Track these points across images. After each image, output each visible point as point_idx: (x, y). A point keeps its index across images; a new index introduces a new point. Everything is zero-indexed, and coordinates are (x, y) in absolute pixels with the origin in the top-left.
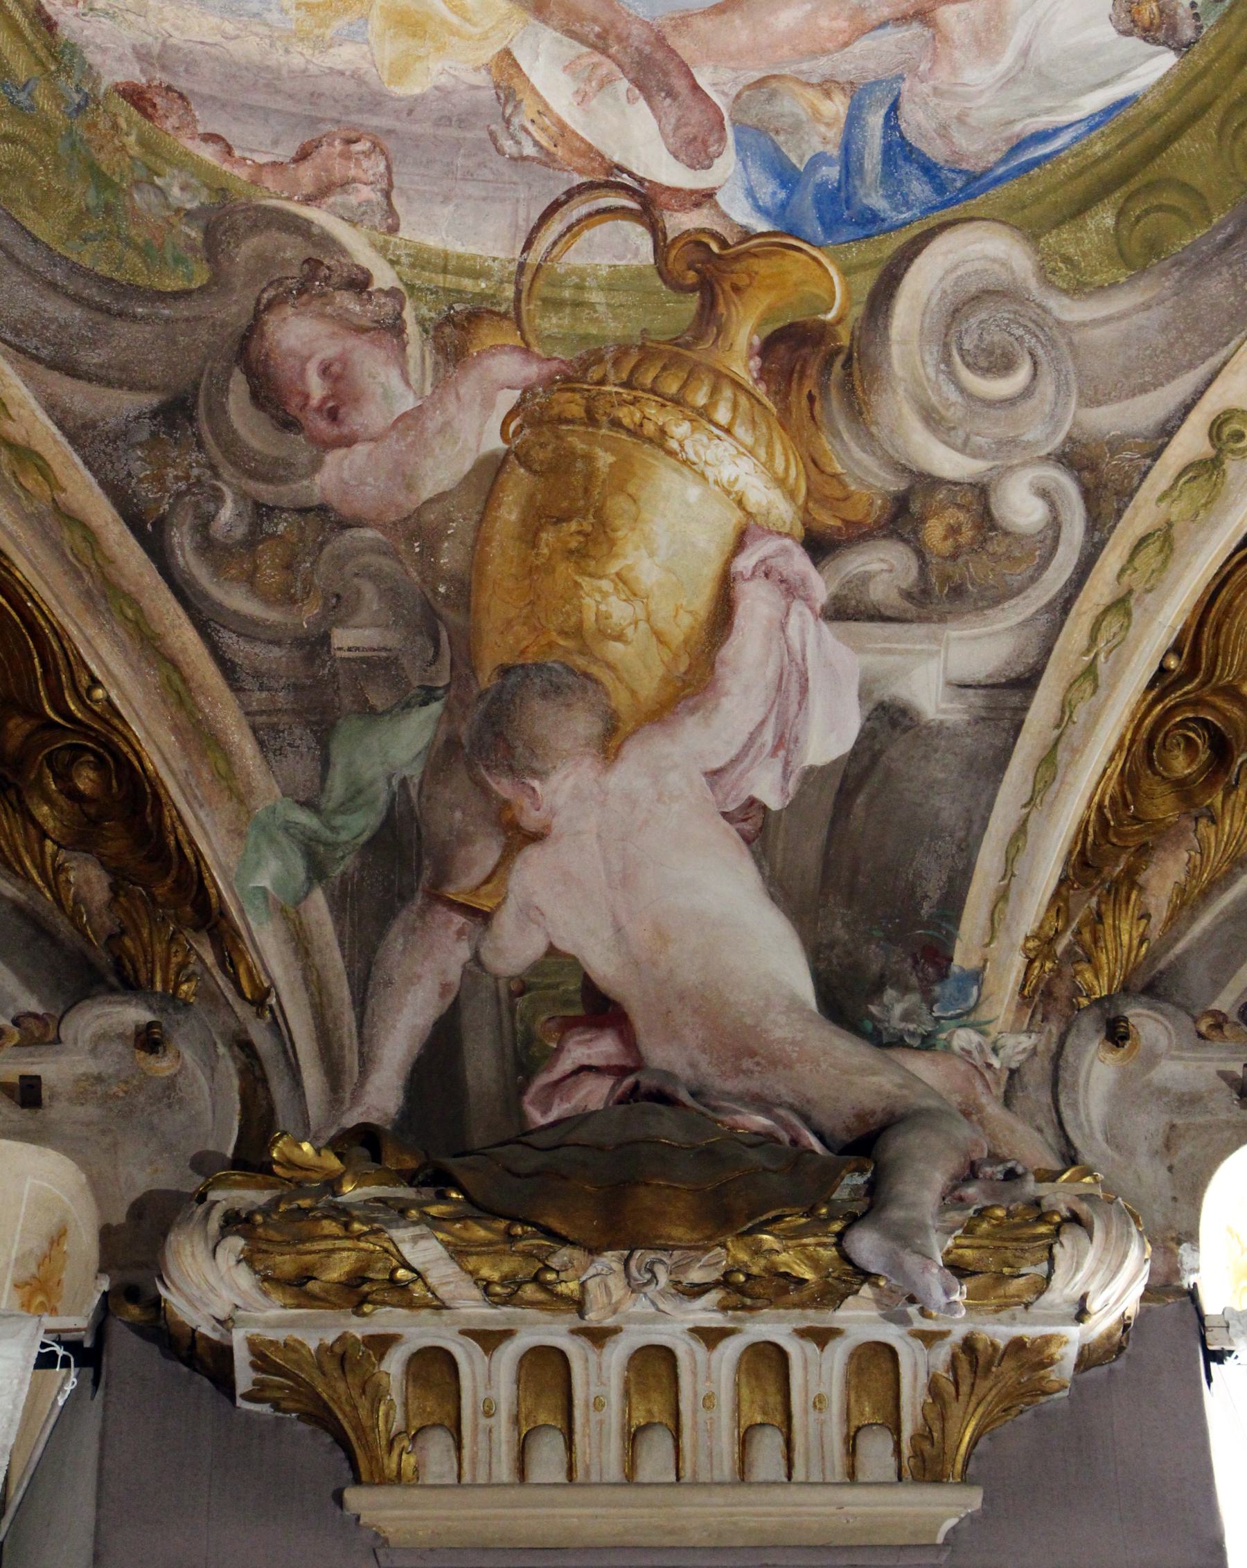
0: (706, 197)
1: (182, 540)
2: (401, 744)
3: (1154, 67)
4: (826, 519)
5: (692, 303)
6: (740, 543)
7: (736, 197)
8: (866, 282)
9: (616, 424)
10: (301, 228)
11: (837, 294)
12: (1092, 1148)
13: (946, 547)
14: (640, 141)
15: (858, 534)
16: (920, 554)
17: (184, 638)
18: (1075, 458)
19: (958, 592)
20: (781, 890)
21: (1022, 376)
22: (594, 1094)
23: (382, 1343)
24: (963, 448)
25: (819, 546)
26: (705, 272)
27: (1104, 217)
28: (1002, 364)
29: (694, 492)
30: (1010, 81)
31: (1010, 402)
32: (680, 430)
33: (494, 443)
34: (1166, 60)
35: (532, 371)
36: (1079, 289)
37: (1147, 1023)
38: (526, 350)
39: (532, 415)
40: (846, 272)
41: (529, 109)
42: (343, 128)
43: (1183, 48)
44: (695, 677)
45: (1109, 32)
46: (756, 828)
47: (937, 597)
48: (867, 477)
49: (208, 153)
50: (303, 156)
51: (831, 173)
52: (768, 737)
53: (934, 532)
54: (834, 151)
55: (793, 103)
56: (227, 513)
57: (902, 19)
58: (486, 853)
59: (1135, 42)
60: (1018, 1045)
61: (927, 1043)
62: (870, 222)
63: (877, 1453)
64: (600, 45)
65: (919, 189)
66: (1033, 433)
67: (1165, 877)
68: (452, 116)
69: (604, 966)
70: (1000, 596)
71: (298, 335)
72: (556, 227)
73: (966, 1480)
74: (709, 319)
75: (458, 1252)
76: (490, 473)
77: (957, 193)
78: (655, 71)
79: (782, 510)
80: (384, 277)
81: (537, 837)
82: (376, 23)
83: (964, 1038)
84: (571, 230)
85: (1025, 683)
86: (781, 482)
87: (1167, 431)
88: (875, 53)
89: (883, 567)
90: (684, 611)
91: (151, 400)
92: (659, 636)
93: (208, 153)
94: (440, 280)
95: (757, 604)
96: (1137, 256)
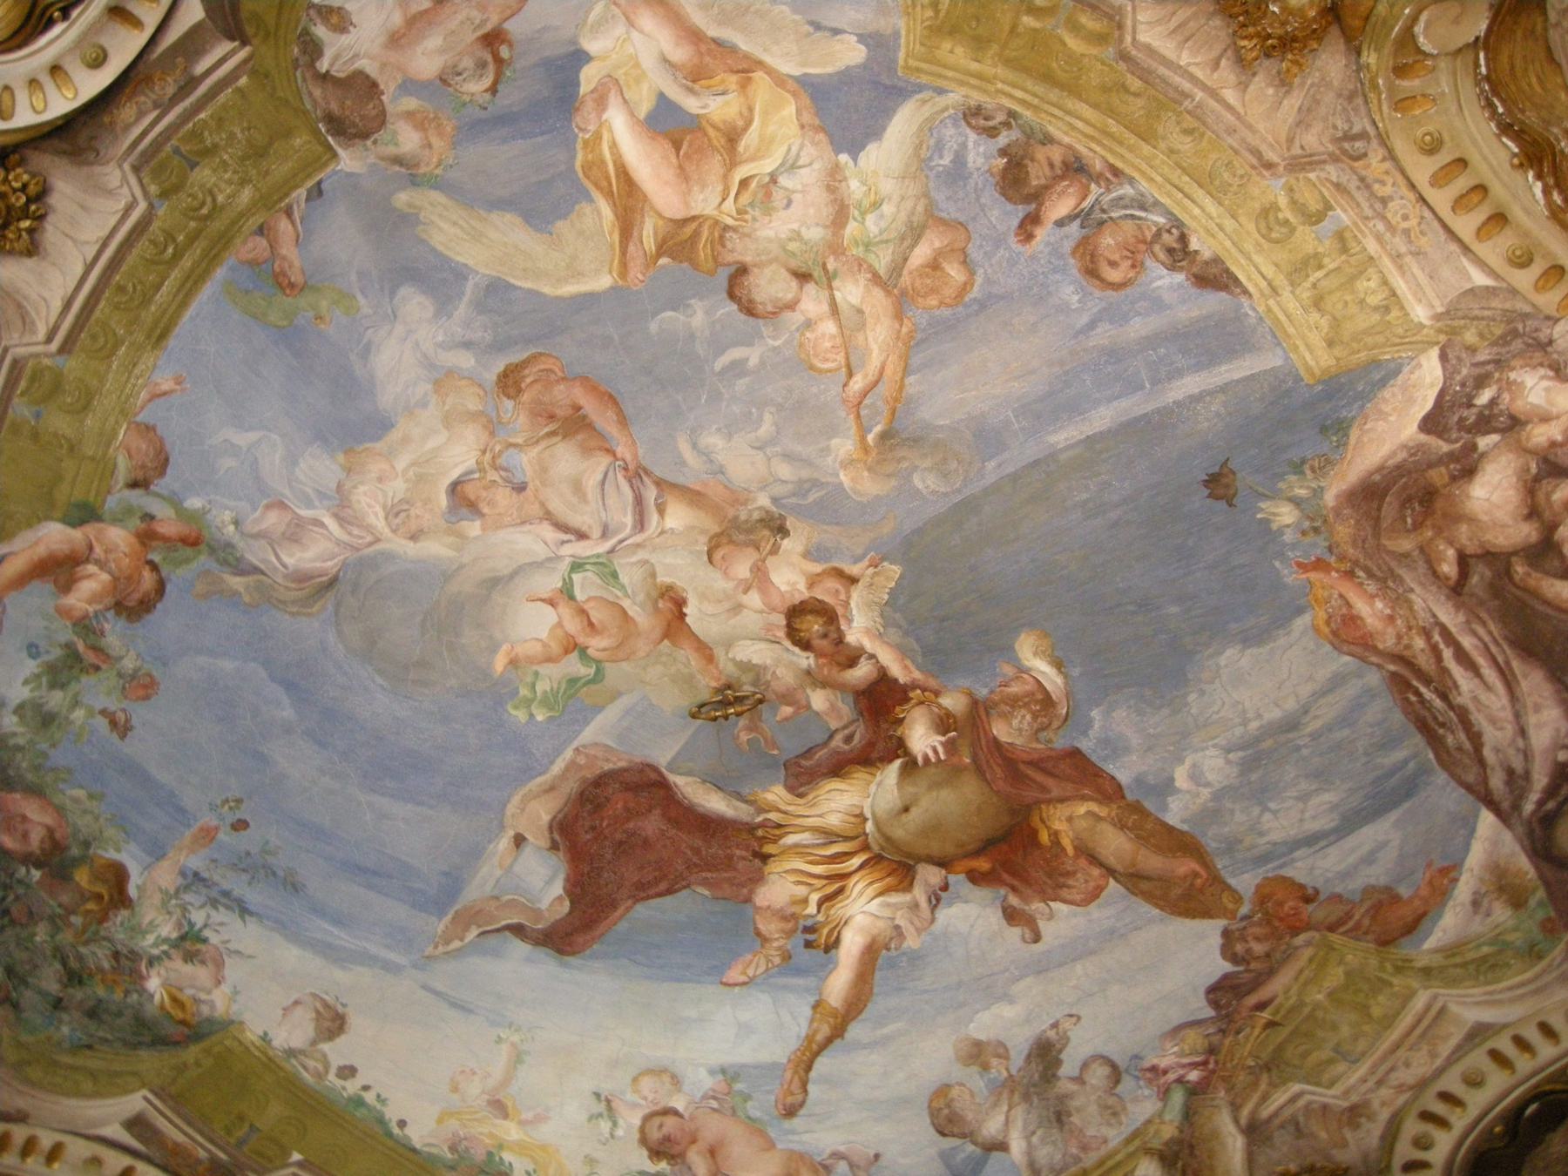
45: (348, 7)
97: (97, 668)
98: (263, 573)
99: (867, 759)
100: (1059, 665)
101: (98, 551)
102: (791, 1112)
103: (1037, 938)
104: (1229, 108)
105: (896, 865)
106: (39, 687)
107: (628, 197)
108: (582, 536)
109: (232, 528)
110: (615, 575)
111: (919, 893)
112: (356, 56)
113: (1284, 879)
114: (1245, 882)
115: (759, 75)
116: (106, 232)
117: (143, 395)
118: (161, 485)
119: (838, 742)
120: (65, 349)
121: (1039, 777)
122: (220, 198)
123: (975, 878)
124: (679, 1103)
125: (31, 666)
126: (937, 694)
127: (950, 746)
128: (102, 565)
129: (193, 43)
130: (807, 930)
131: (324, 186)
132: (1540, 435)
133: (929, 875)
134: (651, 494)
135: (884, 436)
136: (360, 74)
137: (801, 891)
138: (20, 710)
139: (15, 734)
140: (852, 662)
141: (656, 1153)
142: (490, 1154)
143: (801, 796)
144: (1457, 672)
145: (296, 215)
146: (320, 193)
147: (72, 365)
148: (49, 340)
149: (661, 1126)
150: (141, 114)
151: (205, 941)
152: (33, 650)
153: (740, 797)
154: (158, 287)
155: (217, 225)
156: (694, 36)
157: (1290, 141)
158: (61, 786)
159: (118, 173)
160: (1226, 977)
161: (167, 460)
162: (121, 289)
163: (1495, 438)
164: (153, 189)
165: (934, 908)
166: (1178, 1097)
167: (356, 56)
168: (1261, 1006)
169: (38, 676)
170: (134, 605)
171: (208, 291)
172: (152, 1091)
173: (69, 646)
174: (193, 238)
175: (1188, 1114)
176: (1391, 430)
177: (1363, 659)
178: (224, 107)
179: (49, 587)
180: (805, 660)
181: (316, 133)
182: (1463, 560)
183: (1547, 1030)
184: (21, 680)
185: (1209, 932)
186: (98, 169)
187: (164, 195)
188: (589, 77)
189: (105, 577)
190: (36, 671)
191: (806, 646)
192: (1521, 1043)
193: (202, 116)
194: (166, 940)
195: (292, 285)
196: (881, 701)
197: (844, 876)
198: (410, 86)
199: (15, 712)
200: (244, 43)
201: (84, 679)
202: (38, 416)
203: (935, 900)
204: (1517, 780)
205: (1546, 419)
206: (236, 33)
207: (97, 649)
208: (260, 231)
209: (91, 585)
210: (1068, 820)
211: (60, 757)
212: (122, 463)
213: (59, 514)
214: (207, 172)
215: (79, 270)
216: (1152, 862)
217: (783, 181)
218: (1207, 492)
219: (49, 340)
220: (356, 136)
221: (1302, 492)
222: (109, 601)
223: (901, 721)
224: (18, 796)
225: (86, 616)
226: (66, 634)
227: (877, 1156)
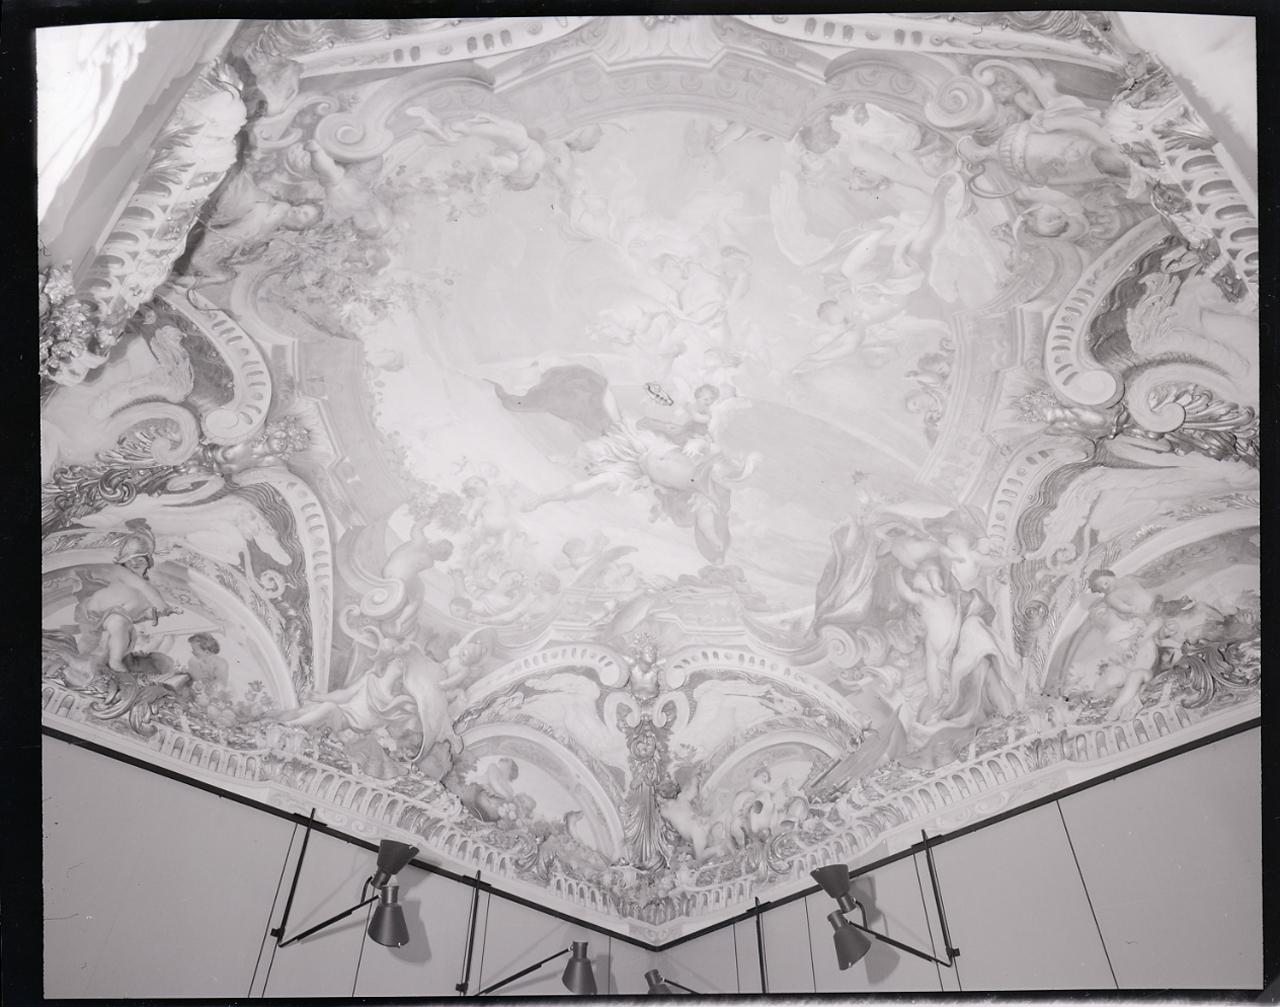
4: (1019, 117)
5: (986, 164)
6: (1037, 133)
7: (955, 168)
8: (957, 134)
13: (1009, 89)
14: (958, 188)
15: (1019, 109)
19: (1018, 82)
21: (957, 92)
28: (956, 97)
31: (966, 93)
32: (1017, 155)
34: (868, 106)
38: (1019, 189)
48: (1003, 113)
53: (1007, 93)
54: (933, 155)
57: (897, 158)
59: (870, 113)
65: (928, 136)
80: (1020, 219)
85: (1030, 60)
87: (947, 55)
89: (1023, 100)
91: (1078, 248)
98: (569, 216)
99: (670, 438)
100: (756, 468)
102: (524, 510)
103: (653, 522)
104: (996, 408)
105: (640, 470)
107: (842, 253)
108: (681, 308)
109: (579, 192)
110: (674, 327)
111: (635, 483)
113: (740, 570)
114: (729, 561)
115: (922, 275)
118: (578, 155)
119: (668, 426)
121: (710, 487)
123: (657, 492)
124: (490, 482)
126: (713, 442)
127: (697, 457)
130: (591, 464)
132: (946, 551)
133: (646, 481)
134: (718, 320)
135: (799, 376)
136: (838, 136)
137: (603, 452)
139: (410, 186)
140: (703, 413)
141: (465, 490)
142: (403, 447)
143: (638, 429)
144: (852, 572)
145: (748, 135)
146: (767, 140)
148: (610, 65)
149: (476, 483)
150: (760, 46)
151: (385, 307)
153: (620, 413)
156: (928, 246)
157: (995, 432)
160: (692, 576)
161: (589, 149)
163: (934, 539)
165: (635, 490)
166: (640, 591)
168: (692, 591)
170: (511, 182)
172: (299, 342)
175: (637, 599)
176: (916, 512)
177: (833, 547)
180: (692, 400)
182: (889, 553)
183: (763, 662)
185: (705, 563)
187: (721, 72)
188: (888, 220)
191: (697, 396)
192: (752, 660)
194: (371, 297)
195: (712, 148)
196: (695, 428)
197: (620, 459)
199: (421, 179)
200: (826, 81)
203: (637, 489)
204: (832, 607)
205: (952, 550)
208: (731, 123)
209: (509, 163)
210: (704, 507)
215: (655, 53)
216: (711, 535)
217: (882, 299)
218: (853, 474)
219: (610, 65)
220: (806, 144)
221: (875, 499)
223: (693, 438)
227: (537, 543)
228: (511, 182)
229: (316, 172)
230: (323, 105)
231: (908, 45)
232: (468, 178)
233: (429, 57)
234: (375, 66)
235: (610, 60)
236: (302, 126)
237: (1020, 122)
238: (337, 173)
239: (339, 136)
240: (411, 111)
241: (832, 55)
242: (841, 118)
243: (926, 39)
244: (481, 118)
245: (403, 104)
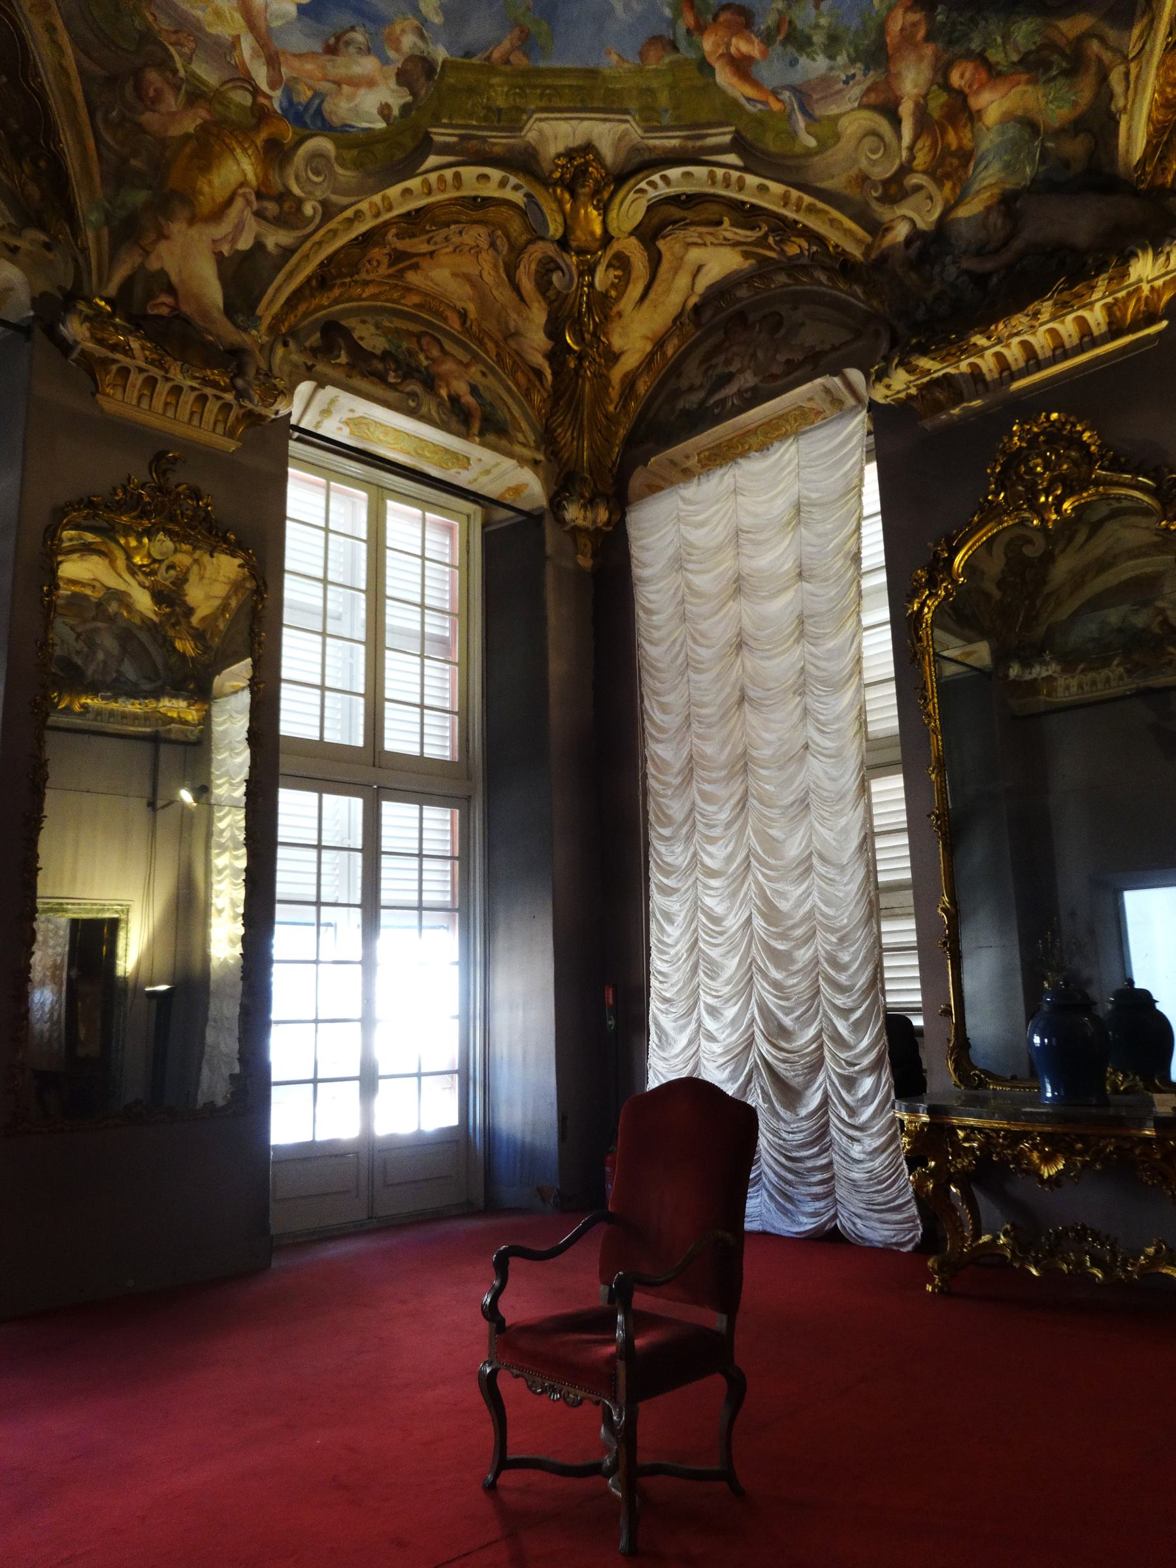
0: (269, 98)
1: (99, 116)
2: (140, 197)
3: (381, 125)
4: (263, 189)
6: (242, 184)
8: (297, 138)
9: (223, 141)
10: (167, 50)
11: (289, 136)
12: (276, 371)
16: (281, 208)
17: (91, 142)
18: (324, 203)
20: (222, 277)
22: (165, 311)
23: (115, 361)
24: (302, 189)
25: (259, 196)
26: (261, 114)
27: (355, 152)
28: (318, 174)
29: (235, 168)
30: (350, 110)
31: (316, 183)
32: (238, 151)
33: (191, 130)
35: (208, 117)
36: (342, 166)
37: (292, 345)
38: (209, 111)
39: (204, 128)
40: (294, 133)
41: (236, 54)
42: (188, 28)
43: (388, 124)
44: (218, 214)
45: (375, 111)
46: (219, 258)
47: (280, 222)
49: (150, 18)
50: (176, 32)
51: (301, 108)
52: (230, 237)
53: (286, 206)
55: (302, 88)
56: (114, 114)
57: (334, 82)
58: (152, 236)
59: (379, 118)
60: (265, 339)
61: (245, 330)
62: (304, 125)
63: (220, 428)
64: (262, 46)
65: (319, 124)
66: (318, 193)
67: (302, 308)
68: (217, 41)
69: (174, 278)
70: (293, 227)
71: (153, 76)
72: (230, 85)
73: (238, 440)
74: (257, 128)
75: (143, 348)
76: (187, 137)
77: (325, 127)
78: (273, 61)
79: (254, 183)
80: (182, 73)
81: (166, 237)
82: (209, 10)
83: (254, 332)
84: (234, 88)
86: (256, 175)
87: (346, 207)
88: (325, 86)
89: (272, 208)
90: (221, 195)
92: (213, 199)
93: (150, 18)
94: (196, 83)
95: (239, 203)
96: (358, 165)
97: (790, 22)
101: (720, 51)
106: (815, 52)
112: (393, 91)
116: (562, 123)
117: (626, 66)
118: (668, 34)
120: (626, 112)
122: (506, 89)
125: (803, 60)
128: (728, 45)
129: (444, 149)
131: (462, 53)
138: (832, 57)
139: (849, 56)
147: (633, 105)
150: (495, 144)
152: (793, 63)
154: (570, 86)
155: (521, 81)
158: (874, 14)
159: (530, 134)
161: (654, 38)
162: (582, 101)
164: (525, 117)
167: (393, 91)
169: (808, 55)
171: (557, 64)
173: (784, 43)
174: (535, 87)
178: (464, 118)
179: (753, 69)
181: (442, 77)
184: (812, 63)
186: (533, 143)
189: (734, 41)
190: (805, 56)
193: (474, 123)
195: (522, 31)
198: (385, 61)
201: (799, 25)
202: (666, 111)
206: (427, 138)
207: (778, 28)
208: (507, 62)
209: (741, 46)
211: (855, 24)
212: (667, 60)
213: (711, 81)
214: (498, 103)
215: (586, 123)
219: (626, 121)
222: (747, 32)
224: (888, 40)
225: (762, 41)
226: (777, 48)
228: (745, 20)
229: (923, 123)
230: (875, 194)
231: (377, 198)
232: (788, 40)
233: (776, 188)
234: (821, 205)
235: (624, 126)
236: (901, 185)
237: (259, 185)
238: (906, 110)
239: (882, 151)
240: (812, 142)
241: (433, 160)
242: (402, 101)
243: (368, 214)
244: (754, 106)
245: (817, 153)
